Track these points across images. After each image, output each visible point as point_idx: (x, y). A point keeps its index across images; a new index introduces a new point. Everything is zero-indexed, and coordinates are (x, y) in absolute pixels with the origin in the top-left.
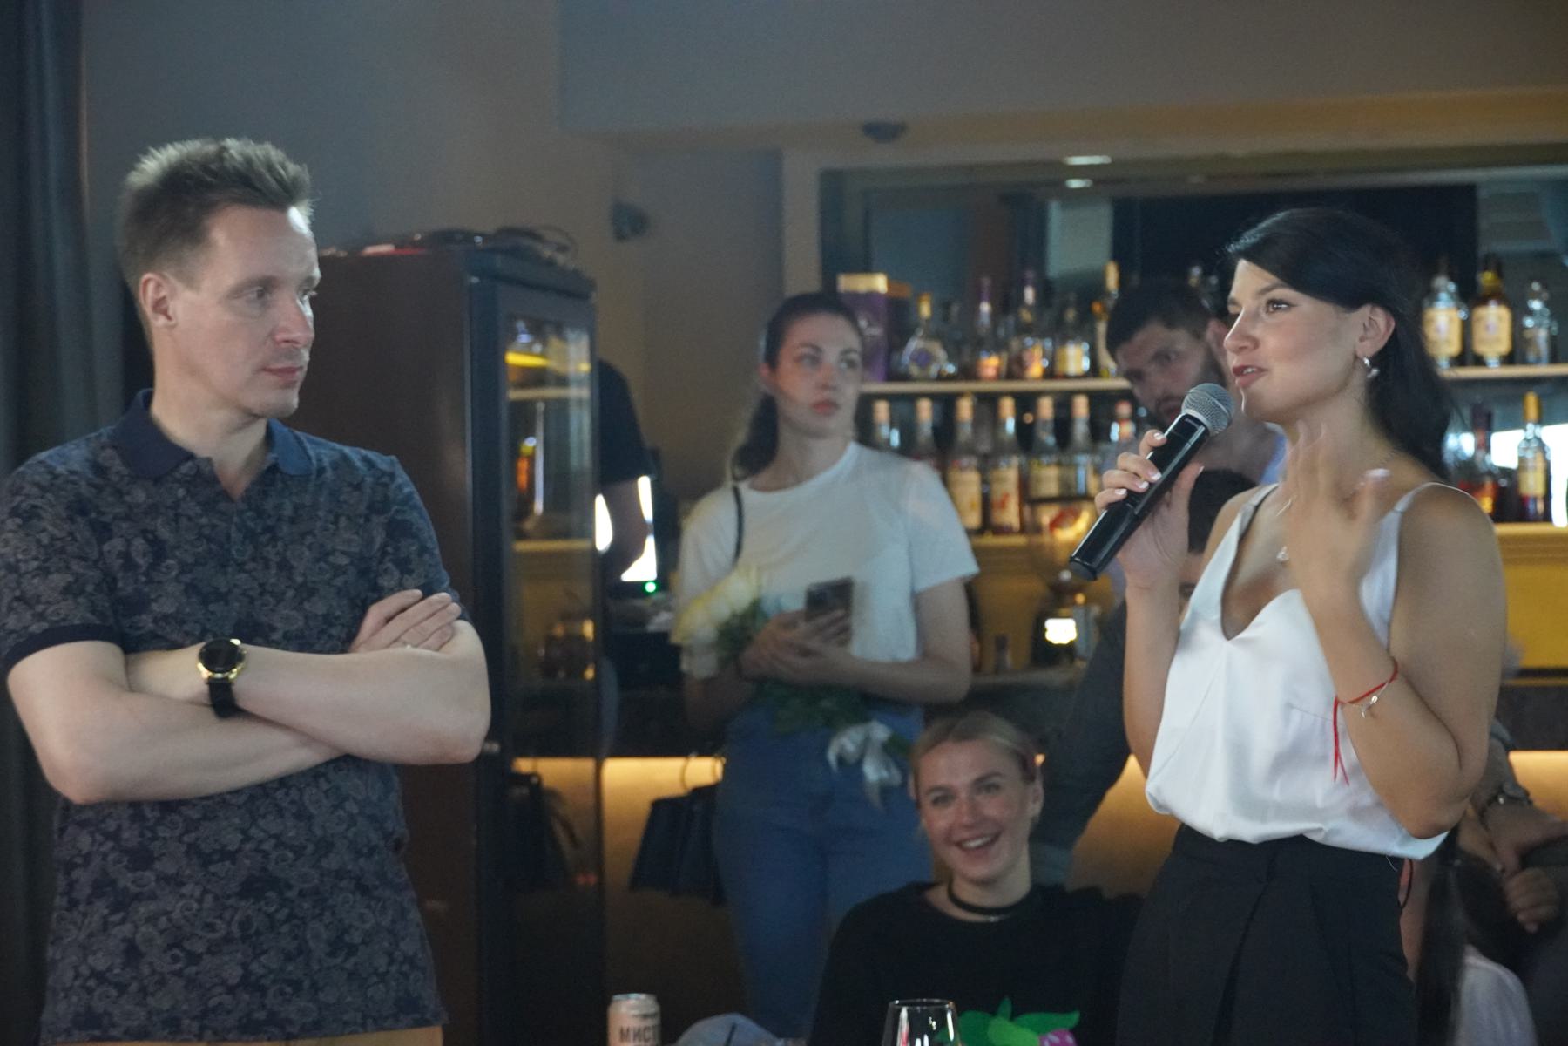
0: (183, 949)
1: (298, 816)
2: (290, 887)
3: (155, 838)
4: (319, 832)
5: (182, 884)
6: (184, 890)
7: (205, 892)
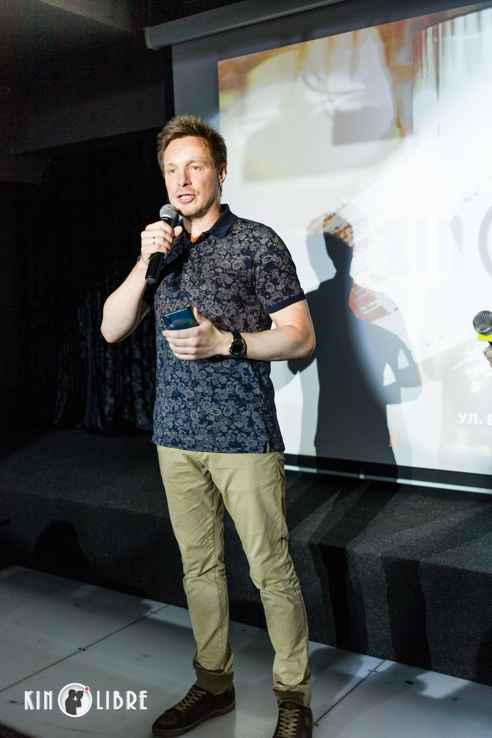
1: (187, 371)
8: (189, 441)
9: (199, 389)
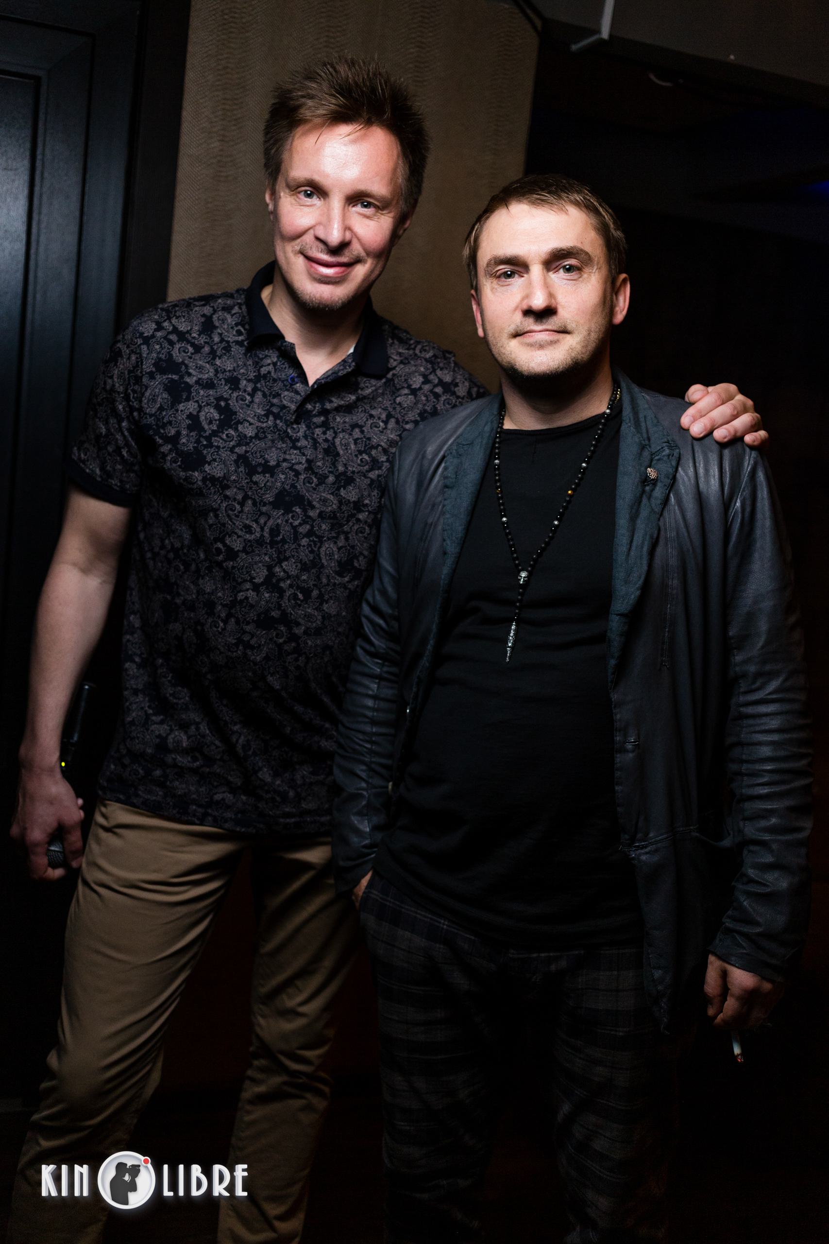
0: (225, 545)
2: (313, 507)
3: (210, 445)
4: (341, 468)
5: (227, 487)
6: (228, 493)
7: (246, 497)
8: (308, 616)
9: (351, 494)
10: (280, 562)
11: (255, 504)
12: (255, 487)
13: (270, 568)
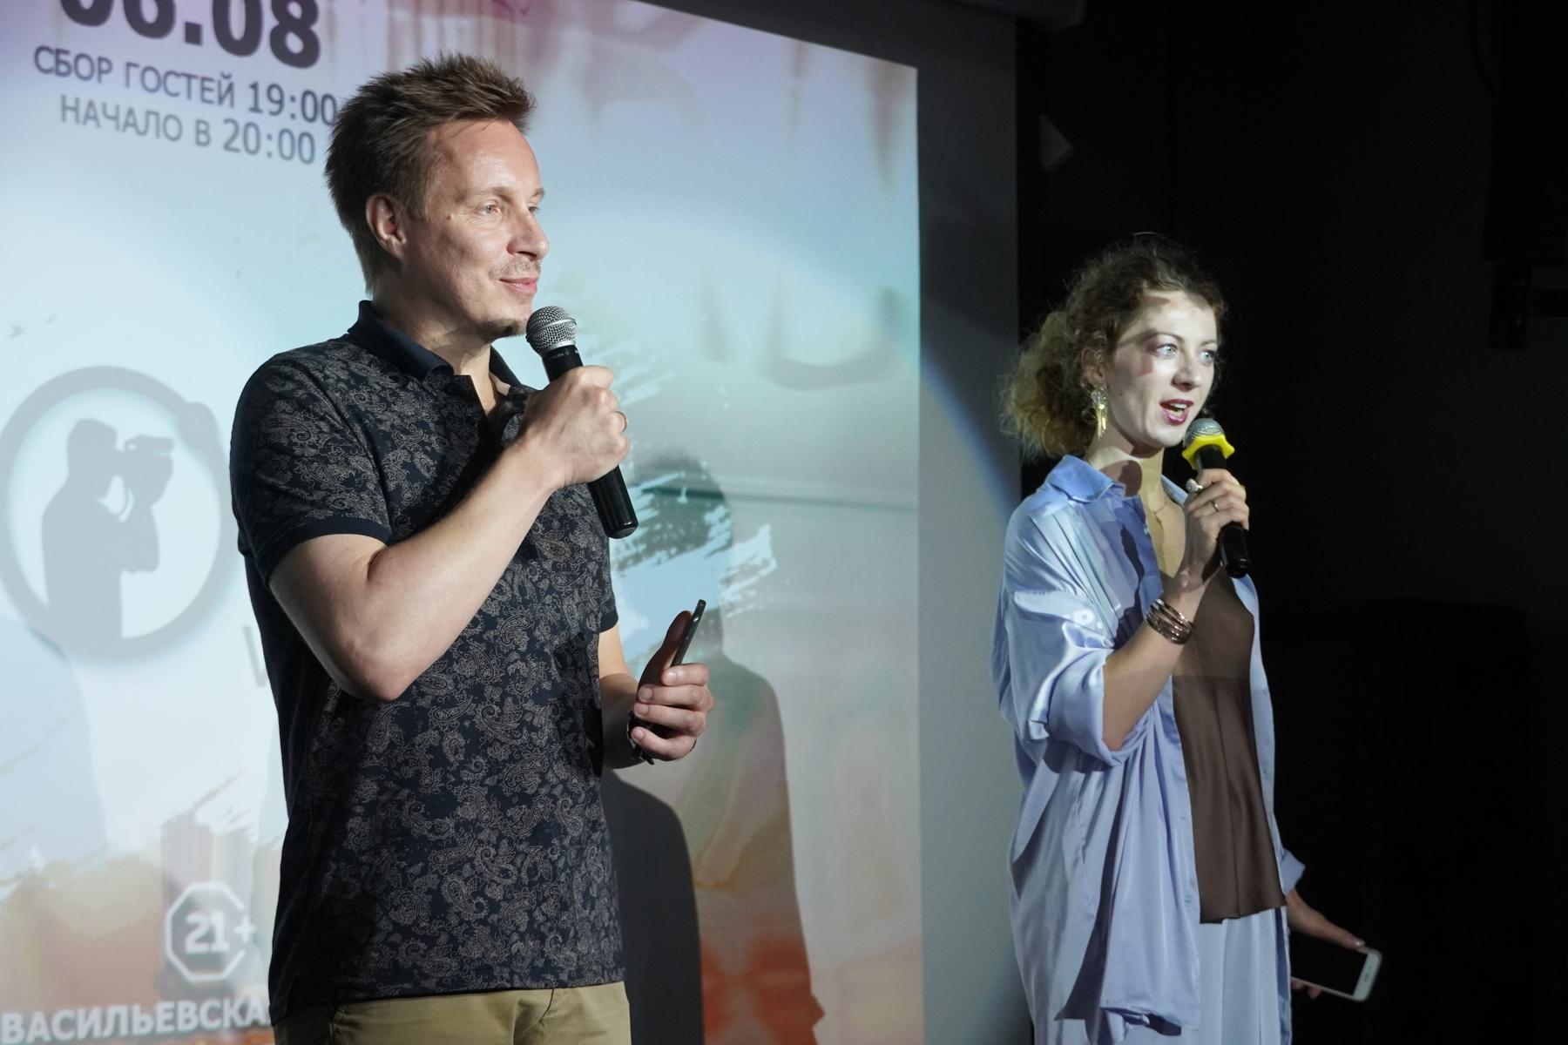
5: (480, 830)
6: (482, 836)
7: (500, 837)
10: (539, 904)
11: (510, 843)
12: (509, 823)
13: (530, 912)
